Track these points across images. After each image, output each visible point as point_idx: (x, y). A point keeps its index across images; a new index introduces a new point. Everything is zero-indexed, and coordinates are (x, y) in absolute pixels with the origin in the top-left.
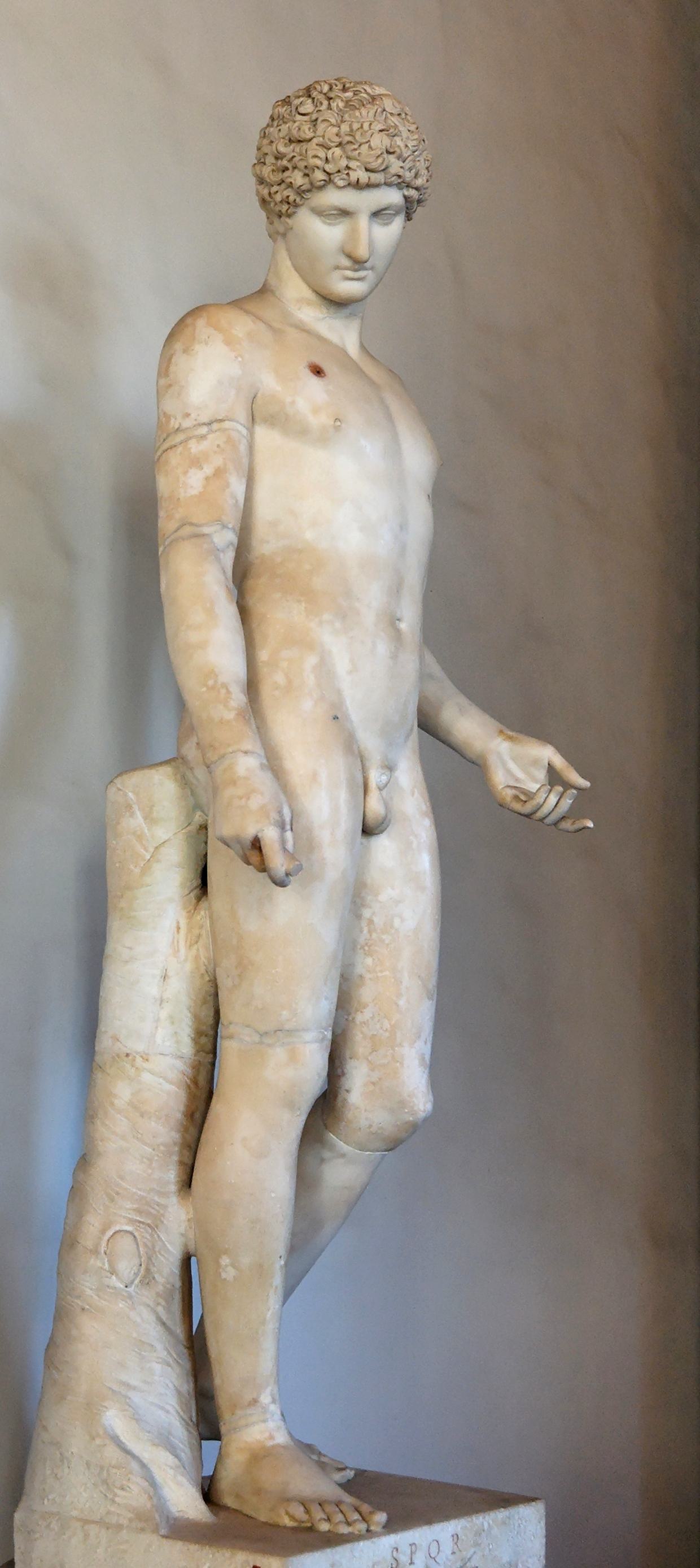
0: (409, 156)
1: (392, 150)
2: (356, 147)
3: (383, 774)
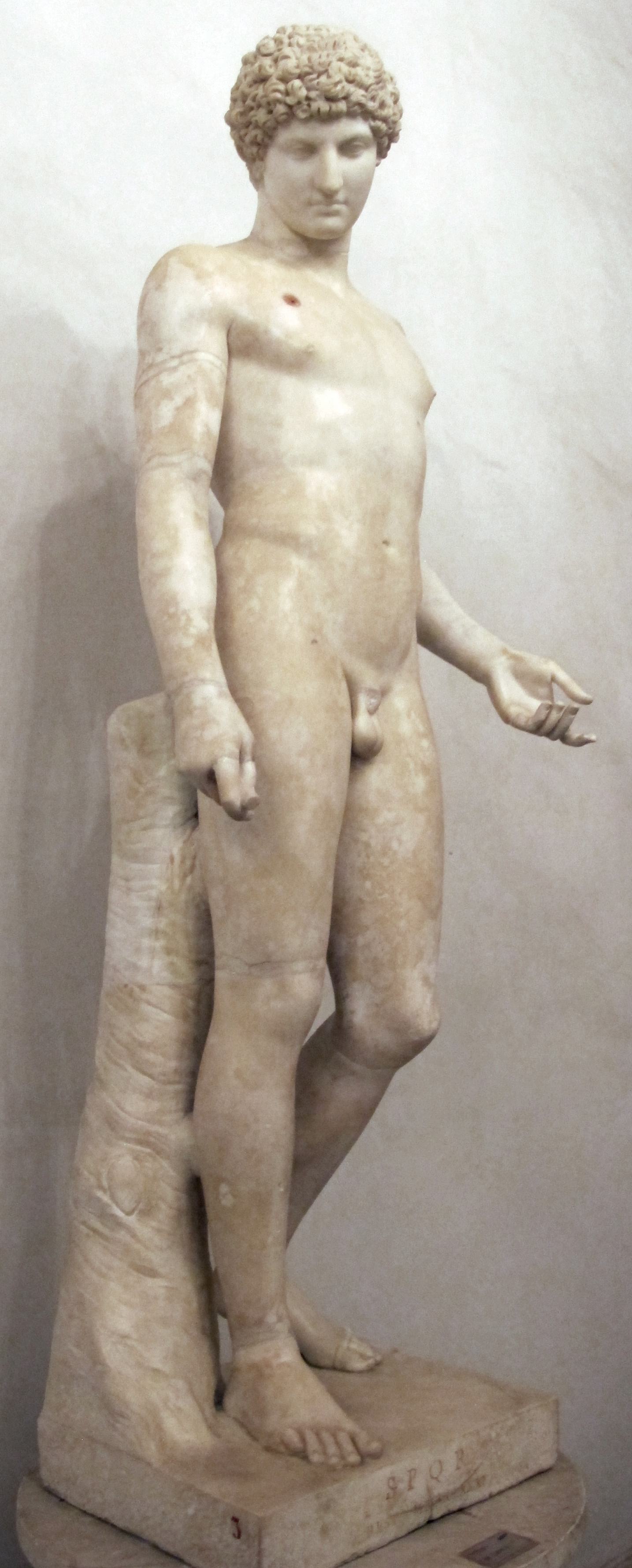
2: (314, 76)
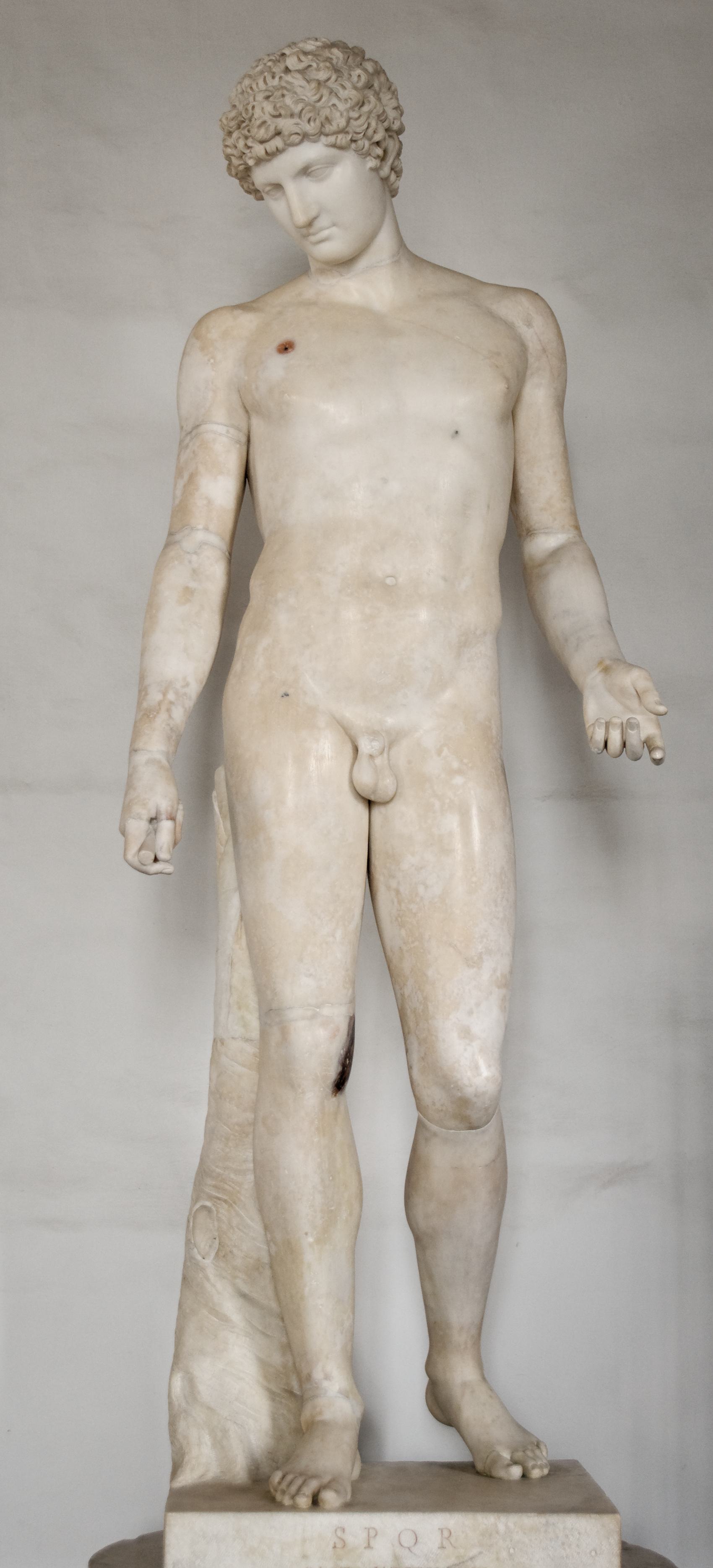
0: (302, 109)
1: (277, 113)
2: (247, 122)
3: (373, 740)
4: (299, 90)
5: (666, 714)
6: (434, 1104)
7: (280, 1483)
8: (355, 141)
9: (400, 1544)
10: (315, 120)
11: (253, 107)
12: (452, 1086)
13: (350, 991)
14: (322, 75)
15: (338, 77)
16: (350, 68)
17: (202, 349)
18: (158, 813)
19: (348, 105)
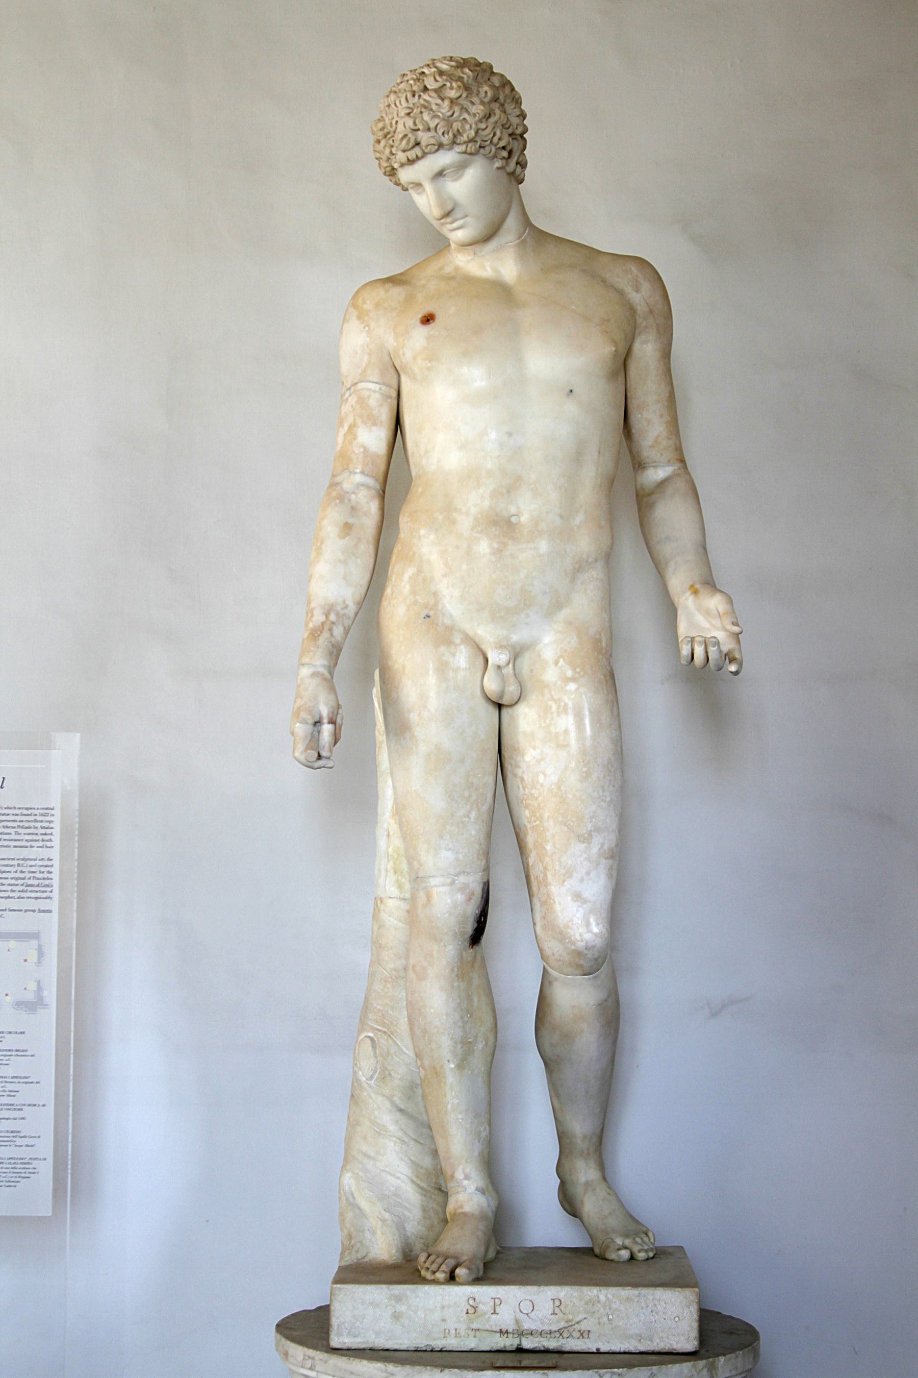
1: (416, 128)
4: (434, 107)
5: (741, 633)
6: (553, 955)
7: (425, 1262)
8: (484, 147)
9: (520, 1311)
10: (448, 132)
11: (397, 122)
12: (567, 941)
13: (484, 862)
14: (453, 94)
15: (468, 94)
16: (480, 85)
17: (359, 318)
18: (321, 718)
19: (477, 118)
